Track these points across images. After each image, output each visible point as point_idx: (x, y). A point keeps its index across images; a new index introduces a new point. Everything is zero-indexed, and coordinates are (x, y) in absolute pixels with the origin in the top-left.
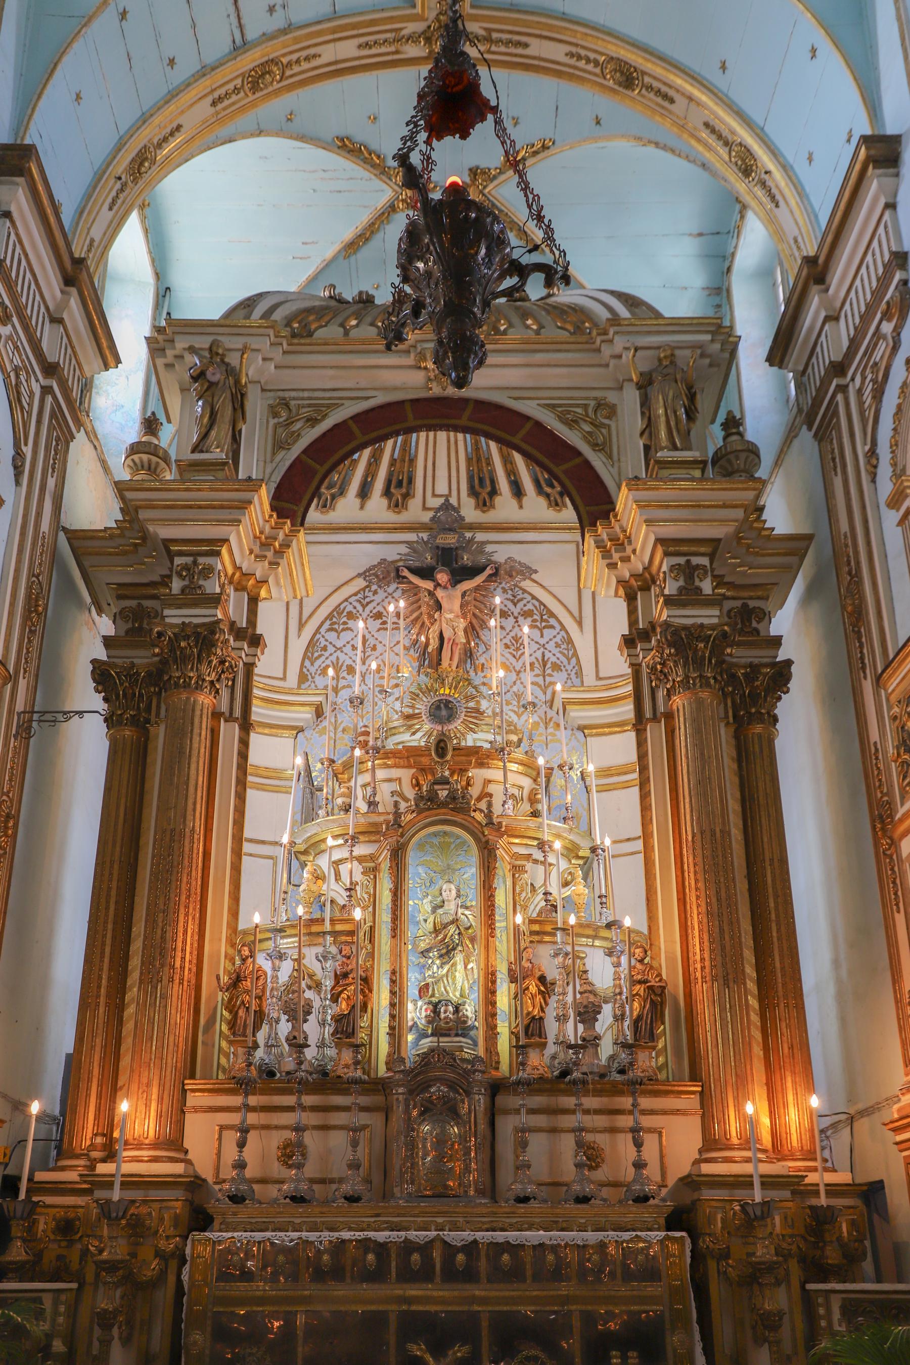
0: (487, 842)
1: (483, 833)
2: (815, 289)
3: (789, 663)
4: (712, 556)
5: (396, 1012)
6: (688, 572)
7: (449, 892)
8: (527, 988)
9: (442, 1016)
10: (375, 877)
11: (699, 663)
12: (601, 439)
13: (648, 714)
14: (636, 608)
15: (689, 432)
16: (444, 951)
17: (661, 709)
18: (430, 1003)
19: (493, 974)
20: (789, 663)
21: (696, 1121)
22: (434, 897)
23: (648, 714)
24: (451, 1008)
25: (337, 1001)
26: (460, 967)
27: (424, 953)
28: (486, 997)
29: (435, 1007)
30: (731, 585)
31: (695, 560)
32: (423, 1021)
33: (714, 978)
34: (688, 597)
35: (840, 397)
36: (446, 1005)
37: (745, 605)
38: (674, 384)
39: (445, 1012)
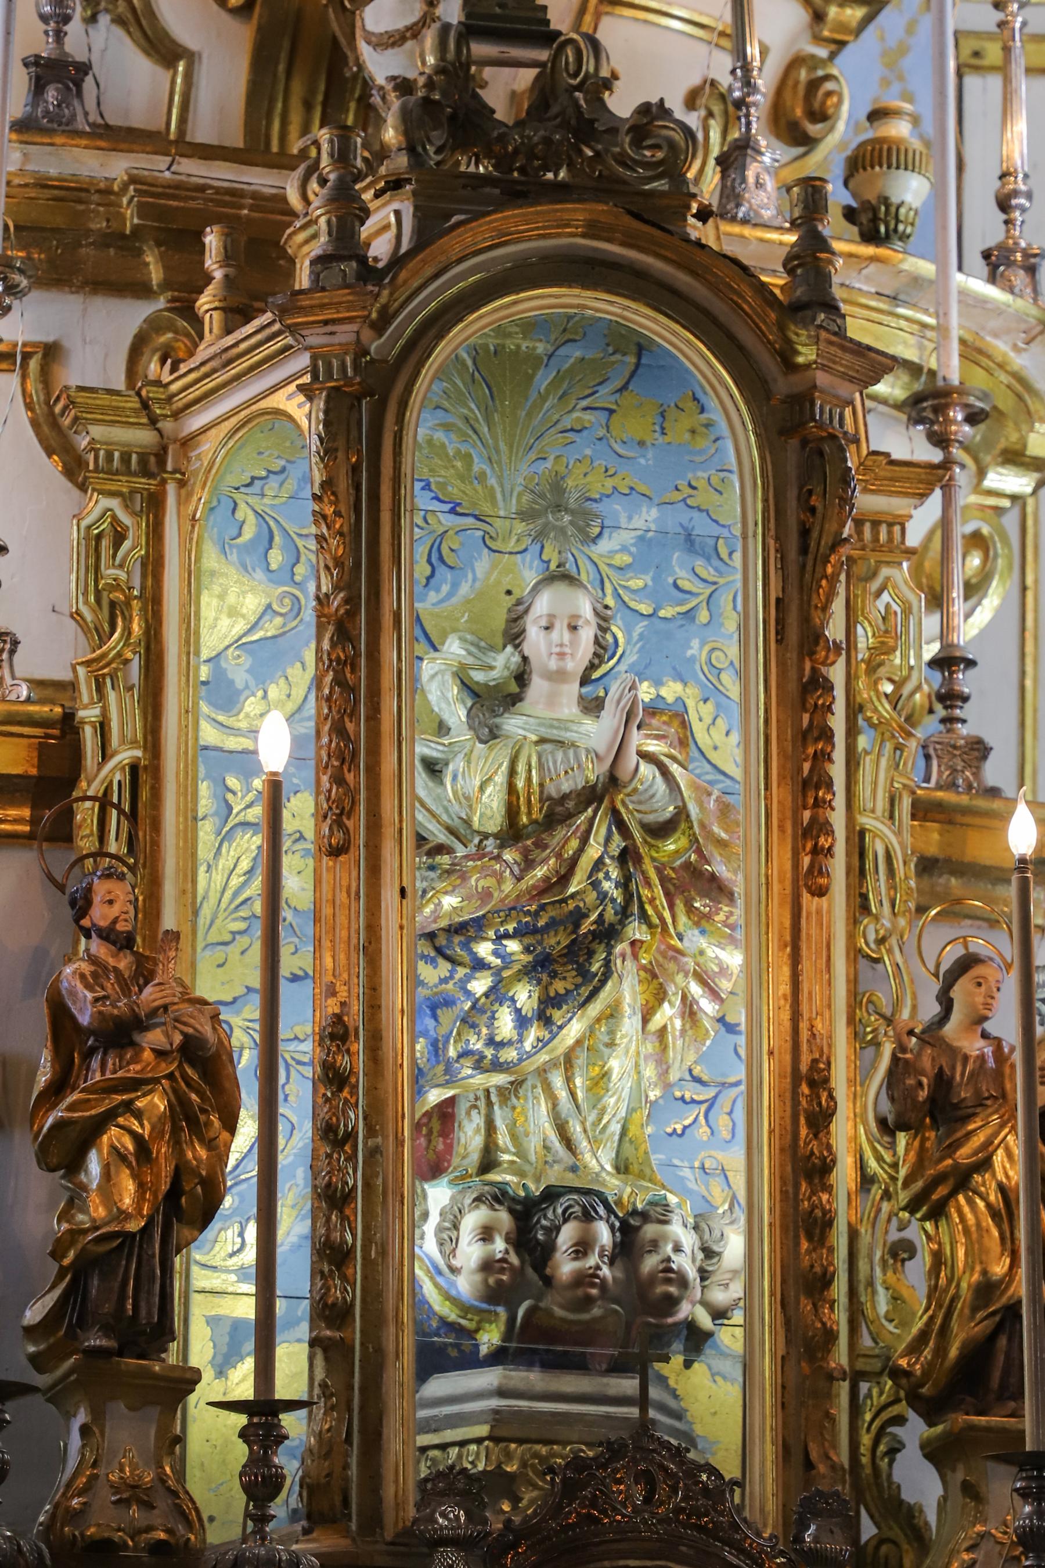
0: (802, 401)
1: (786, 357)
5: (353, 1238)
7: (558, 633)
8: (985, 1164)
9: (566, 1267)
10: (155, 504)
16: (557, 941)
18: (500, 1197)
19: (817, 1079)
22: (481, 645)
24: (604, 1234)
25: (74, 1164)
26: (630, 1024)
27: (449, 941)
28: (787, 1197)
29: (528, 1221)
32: (465, 1285)
36: (587, 1217)
39: (582, 1247)
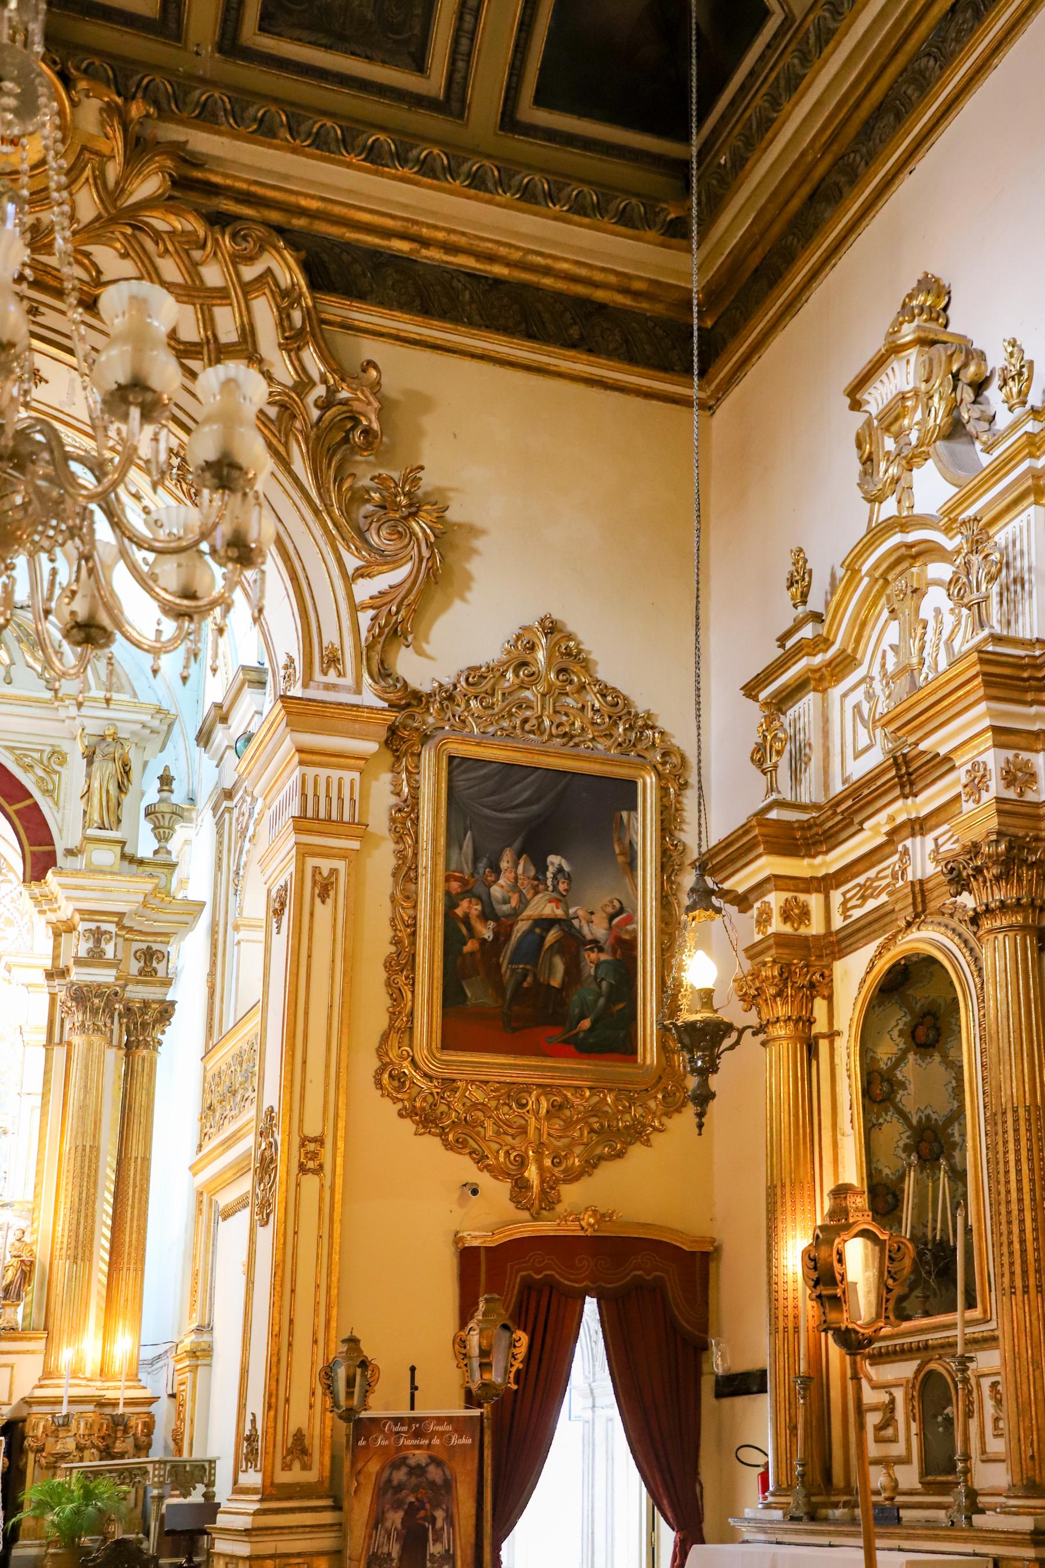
2: (219, 726)
3: (173, 1003)
4: (117, 924)
6: (98, 936)
11: (95, 1012)
12: (50, 787)
13: (56, 1039)
14: (59, 945)
15: (119, 804)
17: (66, 1038)
20: (173, 1003)
21: (40, 1358)
23: (56, 1039)
30: (141, 932)
31: (104, 927)
33: (68, 1257)
34: (95, 958)
35: (227, 816)
37: (149, 948)
38: (111, 765)
